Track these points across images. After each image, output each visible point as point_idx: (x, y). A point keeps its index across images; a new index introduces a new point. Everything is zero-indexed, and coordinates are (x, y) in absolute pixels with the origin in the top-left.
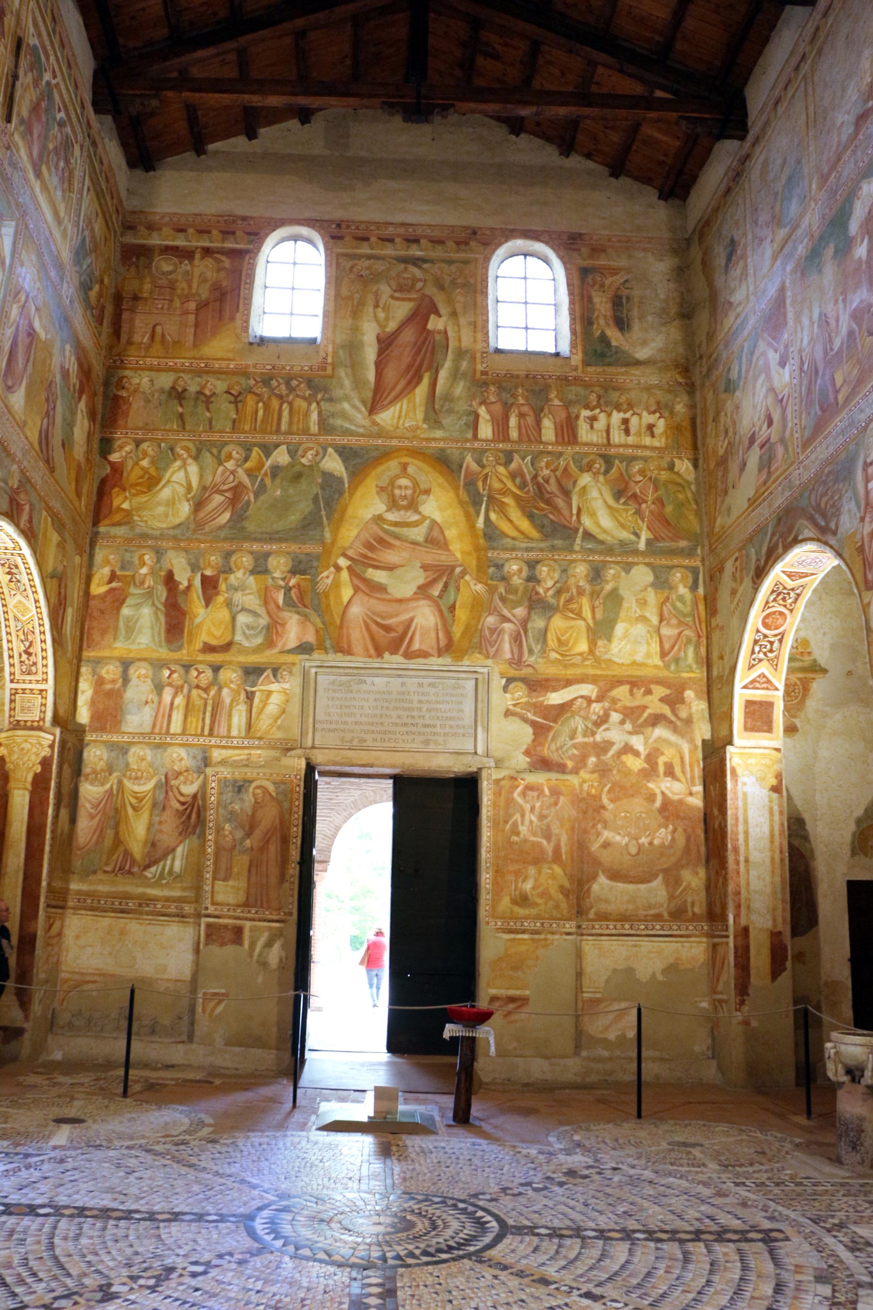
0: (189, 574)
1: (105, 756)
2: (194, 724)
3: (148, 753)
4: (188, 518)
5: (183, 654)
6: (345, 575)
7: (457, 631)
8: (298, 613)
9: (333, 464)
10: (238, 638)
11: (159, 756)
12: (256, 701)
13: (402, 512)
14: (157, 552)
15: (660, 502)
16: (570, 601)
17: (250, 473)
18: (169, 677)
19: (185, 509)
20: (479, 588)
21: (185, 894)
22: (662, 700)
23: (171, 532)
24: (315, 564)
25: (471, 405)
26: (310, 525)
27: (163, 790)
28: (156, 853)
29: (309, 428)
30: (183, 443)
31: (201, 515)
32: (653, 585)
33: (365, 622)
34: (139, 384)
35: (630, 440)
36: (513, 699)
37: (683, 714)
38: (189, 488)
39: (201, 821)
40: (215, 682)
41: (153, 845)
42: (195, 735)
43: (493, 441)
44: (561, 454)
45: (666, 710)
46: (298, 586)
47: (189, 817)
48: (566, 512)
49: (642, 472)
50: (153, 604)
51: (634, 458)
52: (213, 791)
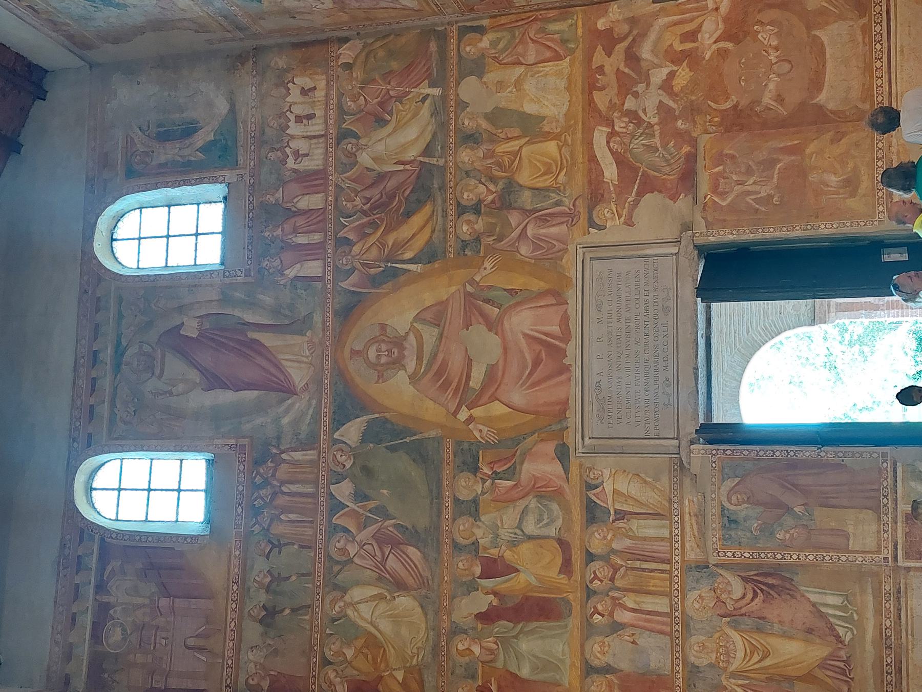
0: (479, 593)
2: (657, 582)
4: (415, 598)
5: (575, 598)
6: (477, 412)
7: (537, 285)
8: (522, 463)
9: (352, 432)
10: (552, 532)
11: (698, 626)
12: (625, 508)
13: (406, 352)
14: (455, 633)
15: (387, 76)
16: (500, 165)
17: (363, 526)
18: (603, 616)
19: (405, 602)
20: (488, 264)
22: (609, 55)
23: (431, 616)
24: (466, 446)
25: (285, 286)
26: (422, 454)
29: (311, 461)
30: (327, 607)
31: (410, 581)
32: (480, 77)
33: (528, 388)
34: (256, 664)
35: (319, 113)
36: (613, 219)
37: (625, 28)
38: (380, 597)
39: (775, 571)
40: (605, 558)
41: (810, 631)
43: (324, 260)
44: (337, 186)
45: (621, 47)
46: (491, 464)
47: (771, 586)
48: (402, 178)
49: (355, 99)
50: (515, 637)
51: (340, 106)
52: (738, 554)
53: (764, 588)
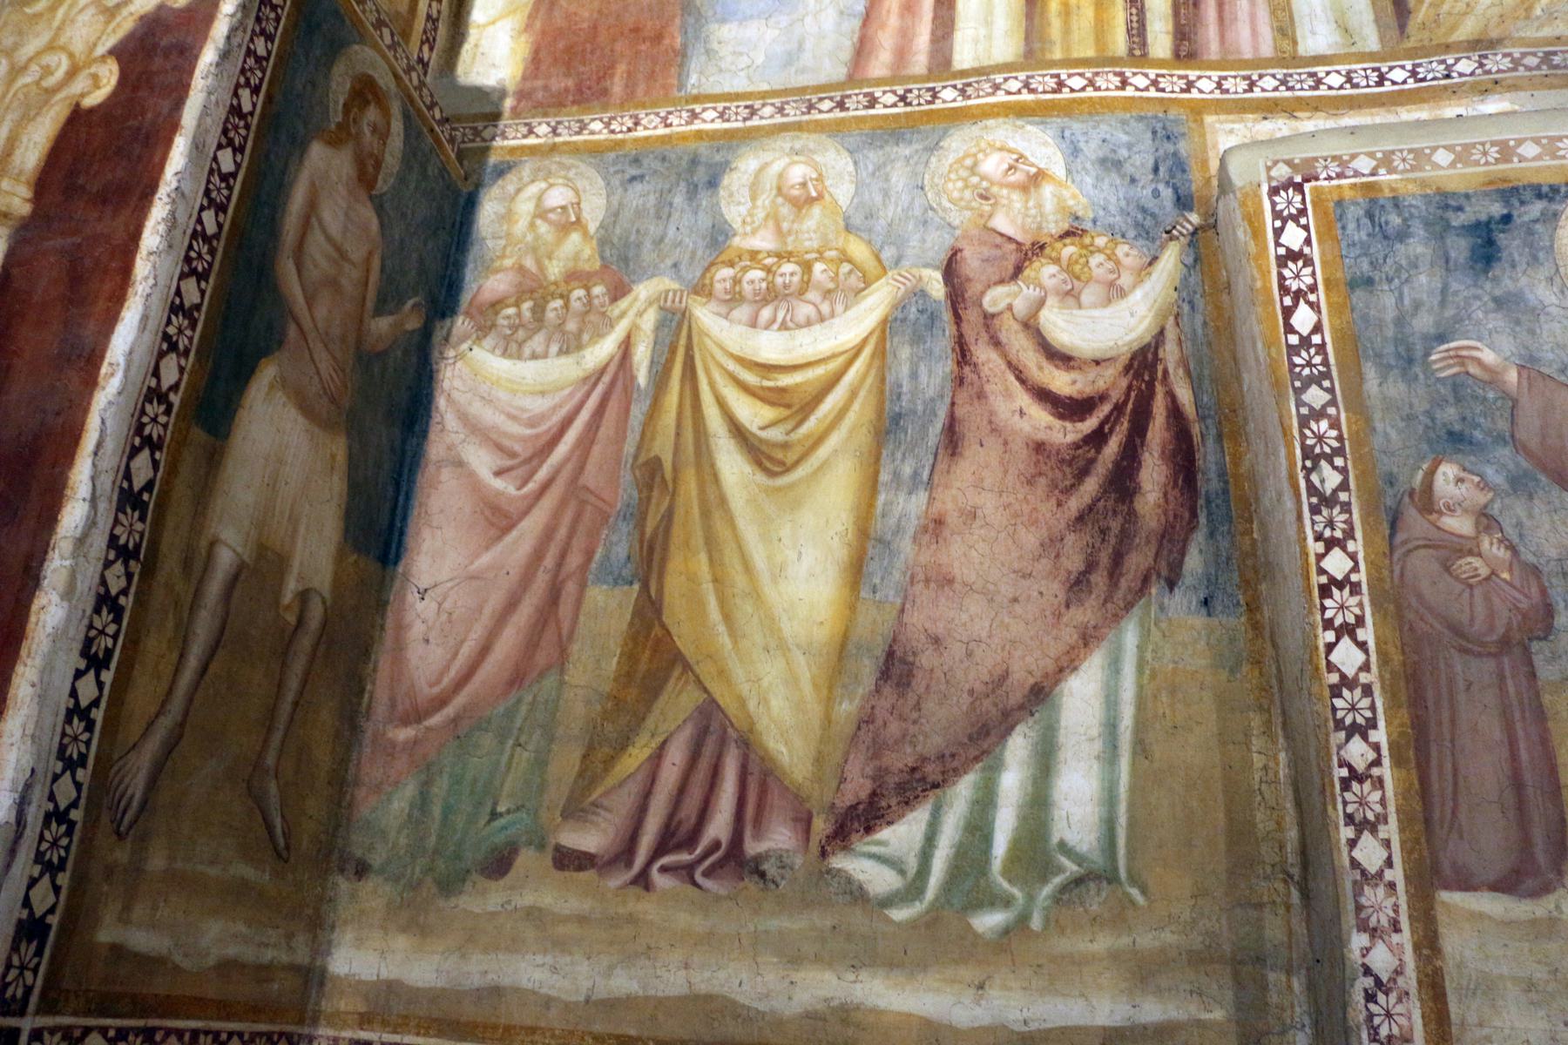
1: (594, 210)
3: (838, 171)
11: (899, 178)
21: (1152, 1011)
27: (943, 343)
28: (916, 727)
41: (896, 668)
42: (1104, 60)
47: (1123, 481)
53: (1112, 447)
